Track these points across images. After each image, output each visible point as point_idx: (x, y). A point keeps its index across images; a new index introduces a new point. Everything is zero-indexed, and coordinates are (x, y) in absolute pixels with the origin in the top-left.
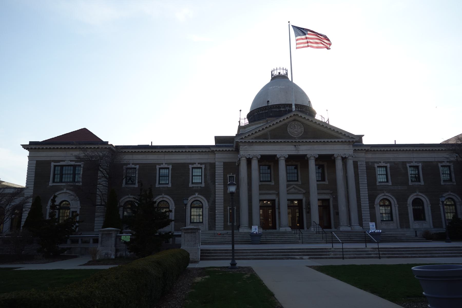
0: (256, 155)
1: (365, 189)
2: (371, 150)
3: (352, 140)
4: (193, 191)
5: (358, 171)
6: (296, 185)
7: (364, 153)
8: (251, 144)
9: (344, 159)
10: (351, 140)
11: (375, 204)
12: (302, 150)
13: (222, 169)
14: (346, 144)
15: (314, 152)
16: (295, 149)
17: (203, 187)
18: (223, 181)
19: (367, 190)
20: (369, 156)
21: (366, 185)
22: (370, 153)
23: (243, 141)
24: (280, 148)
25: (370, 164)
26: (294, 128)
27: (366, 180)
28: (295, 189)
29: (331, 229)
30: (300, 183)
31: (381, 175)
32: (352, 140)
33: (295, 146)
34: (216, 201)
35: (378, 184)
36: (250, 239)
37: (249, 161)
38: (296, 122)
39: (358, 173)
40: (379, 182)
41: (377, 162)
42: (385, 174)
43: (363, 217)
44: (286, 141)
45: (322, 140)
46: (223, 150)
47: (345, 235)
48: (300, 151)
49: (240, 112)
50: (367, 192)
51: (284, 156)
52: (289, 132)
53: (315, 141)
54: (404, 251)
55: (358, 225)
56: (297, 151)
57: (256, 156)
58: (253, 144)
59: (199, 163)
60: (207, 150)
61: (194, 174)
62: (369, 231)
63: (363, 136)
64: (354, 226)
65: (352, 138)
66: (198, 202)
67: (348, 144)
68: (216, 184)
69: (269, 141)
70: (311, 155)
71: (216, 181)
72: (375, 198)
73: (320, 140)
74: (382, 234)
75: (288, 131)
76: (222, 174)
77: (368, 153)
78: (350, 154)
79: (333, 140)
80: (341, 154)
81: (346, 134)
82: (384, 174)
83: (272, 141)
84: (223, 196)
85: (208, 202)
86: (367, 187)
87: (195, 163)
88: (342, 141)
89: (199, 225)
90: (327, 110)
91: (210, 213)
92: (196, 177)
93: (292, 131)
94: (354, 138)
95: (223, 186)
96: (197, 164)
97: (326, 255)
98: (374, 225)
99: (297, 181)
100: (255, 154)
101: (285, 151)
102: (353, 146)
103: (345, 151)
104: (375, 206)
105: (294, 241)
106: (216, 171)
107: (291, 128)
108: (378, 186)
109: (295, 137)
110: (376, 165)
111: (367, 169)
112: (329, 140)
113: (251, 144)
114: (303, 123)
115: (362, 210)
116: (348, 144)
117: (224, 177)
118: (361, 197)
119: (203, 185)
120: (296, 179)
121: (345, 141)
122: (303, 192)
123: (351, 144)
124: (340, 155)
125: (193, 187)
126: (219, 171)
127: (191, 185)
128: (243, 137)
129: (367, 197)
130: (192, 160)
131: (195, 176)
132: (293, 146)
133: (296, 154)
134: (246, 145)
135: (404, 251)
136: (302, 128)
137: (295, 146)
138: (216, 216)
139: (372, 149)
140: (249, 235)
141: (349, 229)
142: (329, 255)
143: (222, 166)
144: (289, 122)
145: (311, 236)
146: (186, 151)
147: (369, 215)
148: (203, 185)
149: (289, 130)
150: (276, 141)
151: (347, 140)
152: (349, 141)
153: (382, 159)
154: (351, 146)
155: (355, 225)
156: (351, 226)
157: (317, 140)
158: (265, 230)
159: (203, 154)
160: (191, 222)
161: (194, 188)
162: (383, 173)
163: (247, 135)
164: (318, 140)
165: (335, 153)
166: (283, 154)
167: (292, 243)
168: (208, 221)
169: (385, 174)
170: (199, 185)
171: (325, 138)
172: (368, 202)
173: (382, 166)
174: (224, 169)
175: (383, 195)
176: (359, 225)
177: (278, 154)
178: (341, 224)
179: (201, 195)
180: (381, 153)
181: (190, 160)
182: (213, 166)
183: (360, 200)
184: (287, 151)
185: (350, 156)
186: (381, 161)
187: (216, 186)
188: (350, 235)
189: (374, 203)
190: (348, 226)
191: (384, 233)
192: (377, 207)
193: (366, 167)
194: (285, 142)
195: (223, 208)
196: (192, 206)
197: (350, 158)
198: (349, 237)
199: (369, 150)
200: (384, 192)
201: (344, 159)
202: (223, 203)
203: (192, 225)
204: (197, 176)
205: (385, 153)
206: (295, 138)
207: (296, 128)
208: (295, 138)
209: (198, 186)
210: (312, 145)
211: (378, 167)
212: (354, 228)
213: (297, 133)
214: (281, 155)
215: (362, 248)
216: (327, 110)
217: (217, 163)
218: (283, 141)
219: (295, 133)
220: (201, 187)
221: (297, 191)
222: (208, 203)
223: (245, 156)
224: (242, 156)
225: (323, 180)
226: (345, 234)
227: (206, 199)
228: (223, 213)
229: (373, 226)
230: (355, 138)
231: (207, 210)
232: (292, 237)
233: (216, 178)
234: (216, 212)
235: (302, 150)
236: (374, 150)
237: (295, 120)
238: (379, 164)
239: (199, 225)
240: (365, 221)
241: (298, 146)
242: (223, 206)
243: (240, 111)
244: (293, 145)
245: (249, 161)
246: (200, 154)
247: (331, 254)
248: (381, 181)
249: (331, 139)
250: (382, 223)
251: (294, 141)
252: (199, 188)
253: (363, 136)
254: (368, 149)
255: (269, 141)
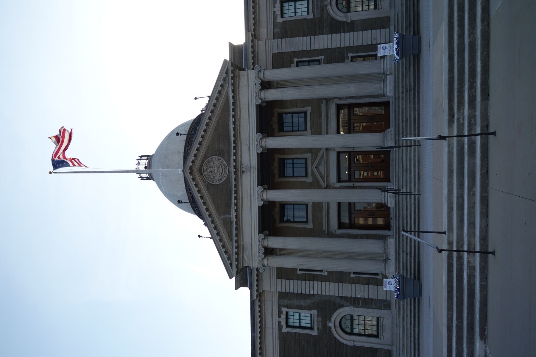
0: (259, 241)
1: (320, 39)
2: (254, 30)
3: (230, 72)
4: (325, 330)
5: (289, 52)
6: (312, 164)
7: (259, 42)
8: (241, 248)
9: (266, 85)
10: (231, 75)
11: (346, 22)
12: (250, 160)
13: (287, 281)
14: (237, 83)
15: (253, 139)
16: (248, 173)
17: (318, 313)
18: (307, 282)
19: (321, 36)
20: (263, 32)
21: (313, 37)
22: (259, 31)
23: (235, 263)
24: (248, 198)
25: (277, 30)
26: (213, 173)
27: (305, 37)
28: (319, 164)
29: (390, 102)
30: (309, 156)
31: (297, 11)
32: (230, 72)
33: (243, 172)
34: (341, 295)
35: (311, 16)
36: (409, 299)
37: (269, 252)
38: (204, 169)
39: (292, 52)
40: (308, 14)
41: (275, 18)
42: (295, 4)
43: (370, 43)
44: (233, 190)
45: (232, 126)
46: (257, 280)
47: (402, 98)
48: (252, 165)
49: (201, 237)
50: (325, 36)
51: (259, 193)
52: (221, 182)
53: (232, 139)
54: (461, 36)
55: (384, 61)
56: (252, 169)
57: (261, 241)
58: (241, 244)
59: (280, 317)
60: (257, 304)
61: (298, 325)
62: (397, 59)
63: (231, 45)
64: (385, 68)
65: (227, 73)
66: (342, 322)
67: (237, 79)
68: (312, 293)
69: (234, 220)
70: (257, 145)
71: (308, 293)
72: (336, 21)
73: (232, 129)
74: (400, 32)
75: (218, 183)
76: (295, 281)
77: (259, 35)
78: (254, 75)
79: (232, 107)
80: (256, 93)
81: (220, 83)
82: (295, 5)
83: (234, 214)
84: (332, 284)
85: (342, 306)
86: (317, 37)
87: (280, 323)
88: (233, 91)
89: (381, 324)
90: (196, 99)
91: (360, 305)
92: (302, 321)
93: (219, 176)
94: (227, 69)
95: (316, 283)
96: (280, 319)
97: (471, 276)
98: (382, 45)
99: (306, 159)
100: (258, 243)
101: (252, 190)
102: (260, 41)
103: (250, 85)
104: (349, 21)
105: (415, 205)
106: (292, 291)
107: (213, 177)
108: (314, 15)
109: (227, 171)
110: (279, 20)
111: (286, 37)
112: (232, 113)
113: (241, 248)
114: (205, 157)
115: (356, 44)
116: (237, 79)
117: (301, 280)
118: (334, 46)
119: (315, 312)
120: (303, 161)
121: (233, 85)
122: (325, 152)
123: (237, 74)
124: (257, 95)
125: (318, 329)
126: (292, 287)
127: (315, 333)
128: (229, 262)
129: (334, 35)
130: (274, 327)
131: (300, 323)
132: (244, 176)
133: (256, 170)
134: (243, 256)
135: (461, 36)
136: (214, 159)
137: (244, 173)
138: (366, 297)
139: (252, 27)
140: (401, 302)
141: (390, 79)
142: (472, 269)
143: (284, 281)
144: (204, 181)
145: (405, 164)
146: (260, 338)
147: (365, 32)
148: (315, 312)
149: (218, 181)
150: (234, 208)
151: (231, 81)
152: (233, 78)
153: (268, 9)
154: (242, 73)
155: (382, 66)
156: (384, 73)
157: (232, 135)
158: (392, 219)
159: (265, 309)
160: (377, 336)
161: (320, 327)
162: (293, 7)
163: (225, 255)
164: (232, 133)
165: (254, 102)
166: (257, 194)
167: (419, 212)
168: (374, 309)
169: (295, 4)
170: (315, 319)
171: (228, 121)
172: (343, 34)
173: (280, 9)
174: (287, 279)
175: (329, 6)
176: (383, 132)
177: (257, 203)
178: (380, 92)
179: (331, 316)
180: (259, 12)
181: (274, 330)
182: (282, 295)
183: (340, 48)
184: (252, 187)
185: (258, 76)
186: (273, 11)
187: (316, 293)
188: (402, 87)
189: (343, 23)
190: (384, 81)
191: (400, 15)
192: (352, 17)
193: (282, 38)
194: (236, 192)
195: (353, 285)
196: (349, 330)
197: (262, 76)
198: (406, 91)
199: (253, 33)
200: (326, 6)
201: (266, 85)
202: (345, 285)
203: (381, 335)
204: (300, 319)
205: (259, 4)
206: (230, 172)
207: (213, 169)
208: (230, 172)
209: (317, 320)
210: (241, 143)
211: (282, 16)
212: (389, 69)
213: (221, 168)
214: (258, 198)
215: (450, 153)
216: (196, 99)
217: (279, 290)
218: (233, 195)
219: (221, 172)
220: (318, 316)
221: (323, 162)
222: (344, 307)
223: (261, 260)
224: (261, 265)
225: (319, 61)
226: (400, 92)
227: (338, 309)
228: (362, 286)
229: (384, 48)
230: (226, 68)
231: (355, 309)
232: (405, 202)
233: (303, 292)
234: (359, 296)
235: (250, 160)
236: (254, 24)
237: (200, 171)
238: (277, 15)
239: (381, 324)
240: (376, 39)
241: (243, 168)
242: (349, 285)
243: (199, 236)
244: (241, 176)
245: (269, 252)
246: (265, 314)
247: (468, 262)
248: (306, 9)
249: (229, 111)
250: (380, 7)
251: (233, 176)
252: (320, 319)
253: (231, 45)
254: (252, 36)
255: (234, 220)
